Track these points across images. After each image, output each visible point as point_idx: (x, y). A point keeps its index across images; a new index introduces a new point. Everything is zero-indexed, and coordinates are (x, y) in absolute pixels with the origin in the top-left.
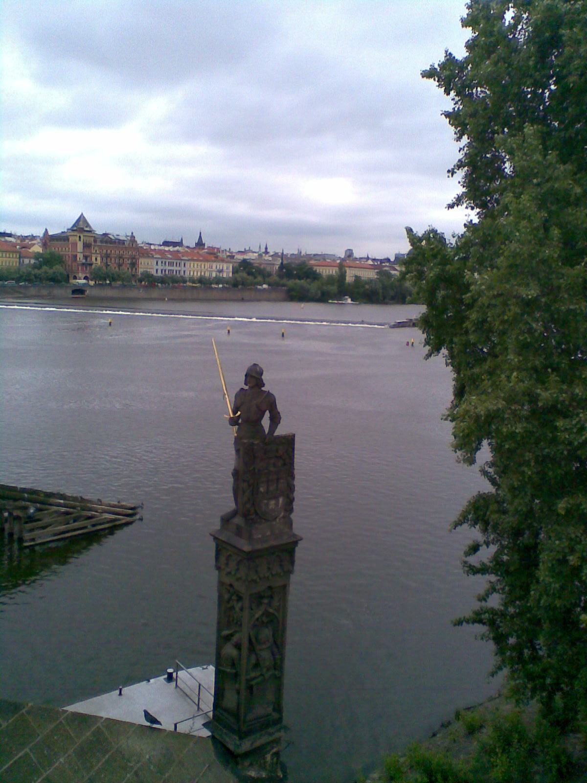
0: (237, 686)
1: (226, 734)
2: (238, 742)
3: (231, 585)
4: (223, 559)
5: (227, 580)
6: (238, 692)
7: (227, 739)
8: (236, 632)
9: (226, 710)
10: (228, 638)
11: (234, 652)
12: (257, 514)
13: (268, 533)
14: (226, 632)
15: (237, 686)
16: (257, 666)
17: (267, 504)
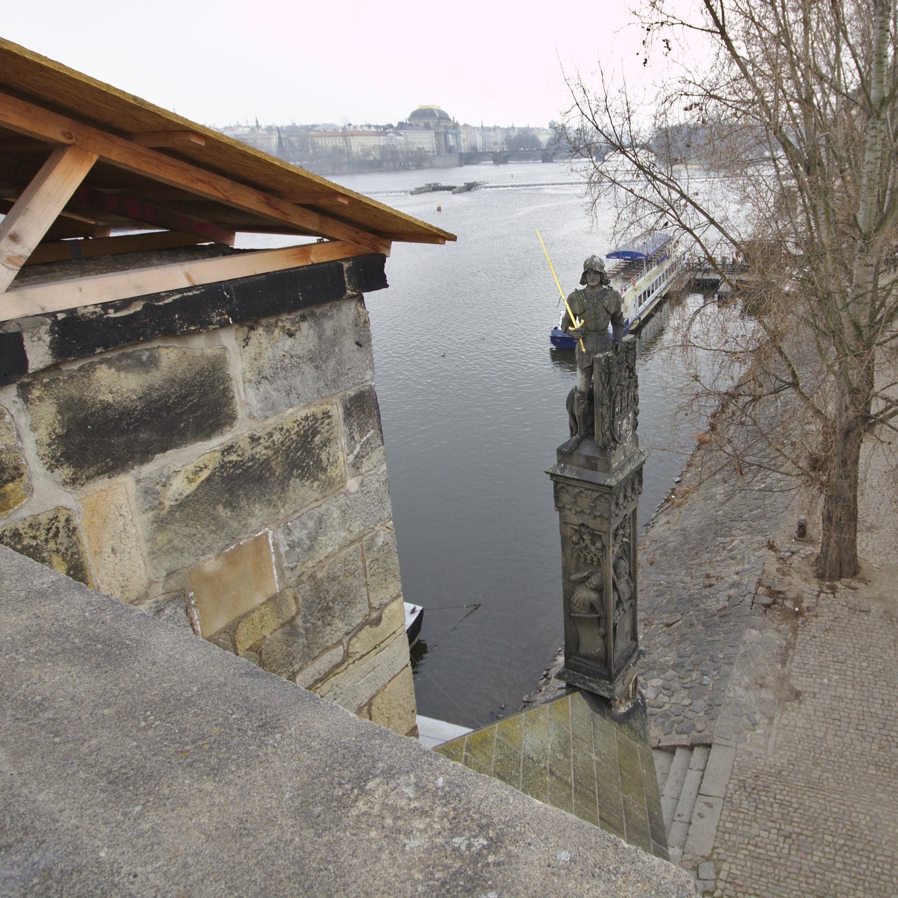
0: (602, 630)
1: (590, 681)
2: (610, 687)
3: (583, 525)
4: (566, 498)
5: (574, 520)
6: (605, 637)
7: (595, 686)
8: (592, 574)
9: (585, 657)
10: (583, 581)
11: (593, 596)
12: (614, 439)
13: (623, 458)
14: (574, 577)
15: (602, 630)
16: (619, 602)
17: (621, 426)
